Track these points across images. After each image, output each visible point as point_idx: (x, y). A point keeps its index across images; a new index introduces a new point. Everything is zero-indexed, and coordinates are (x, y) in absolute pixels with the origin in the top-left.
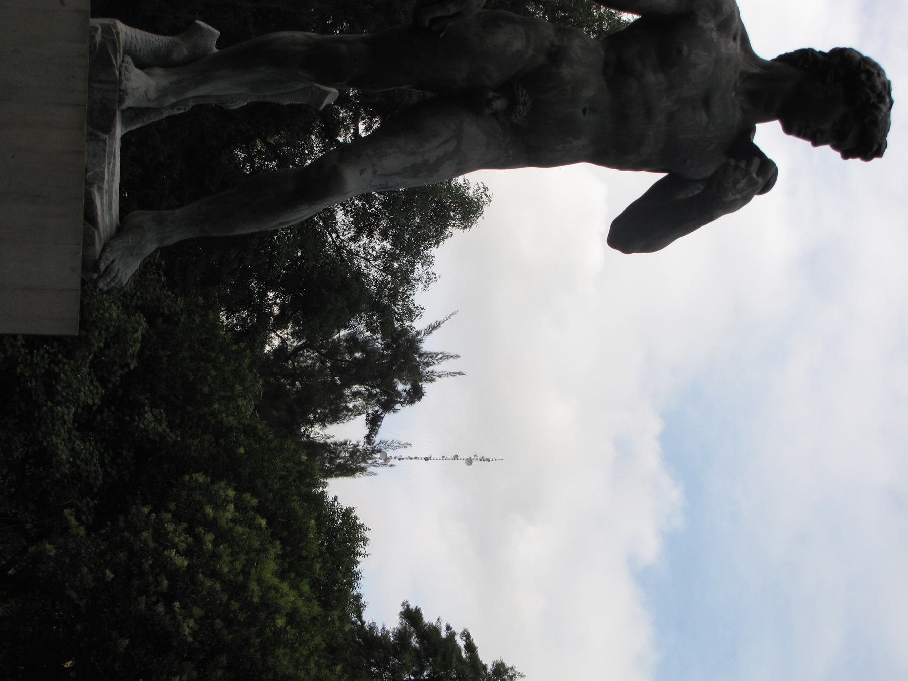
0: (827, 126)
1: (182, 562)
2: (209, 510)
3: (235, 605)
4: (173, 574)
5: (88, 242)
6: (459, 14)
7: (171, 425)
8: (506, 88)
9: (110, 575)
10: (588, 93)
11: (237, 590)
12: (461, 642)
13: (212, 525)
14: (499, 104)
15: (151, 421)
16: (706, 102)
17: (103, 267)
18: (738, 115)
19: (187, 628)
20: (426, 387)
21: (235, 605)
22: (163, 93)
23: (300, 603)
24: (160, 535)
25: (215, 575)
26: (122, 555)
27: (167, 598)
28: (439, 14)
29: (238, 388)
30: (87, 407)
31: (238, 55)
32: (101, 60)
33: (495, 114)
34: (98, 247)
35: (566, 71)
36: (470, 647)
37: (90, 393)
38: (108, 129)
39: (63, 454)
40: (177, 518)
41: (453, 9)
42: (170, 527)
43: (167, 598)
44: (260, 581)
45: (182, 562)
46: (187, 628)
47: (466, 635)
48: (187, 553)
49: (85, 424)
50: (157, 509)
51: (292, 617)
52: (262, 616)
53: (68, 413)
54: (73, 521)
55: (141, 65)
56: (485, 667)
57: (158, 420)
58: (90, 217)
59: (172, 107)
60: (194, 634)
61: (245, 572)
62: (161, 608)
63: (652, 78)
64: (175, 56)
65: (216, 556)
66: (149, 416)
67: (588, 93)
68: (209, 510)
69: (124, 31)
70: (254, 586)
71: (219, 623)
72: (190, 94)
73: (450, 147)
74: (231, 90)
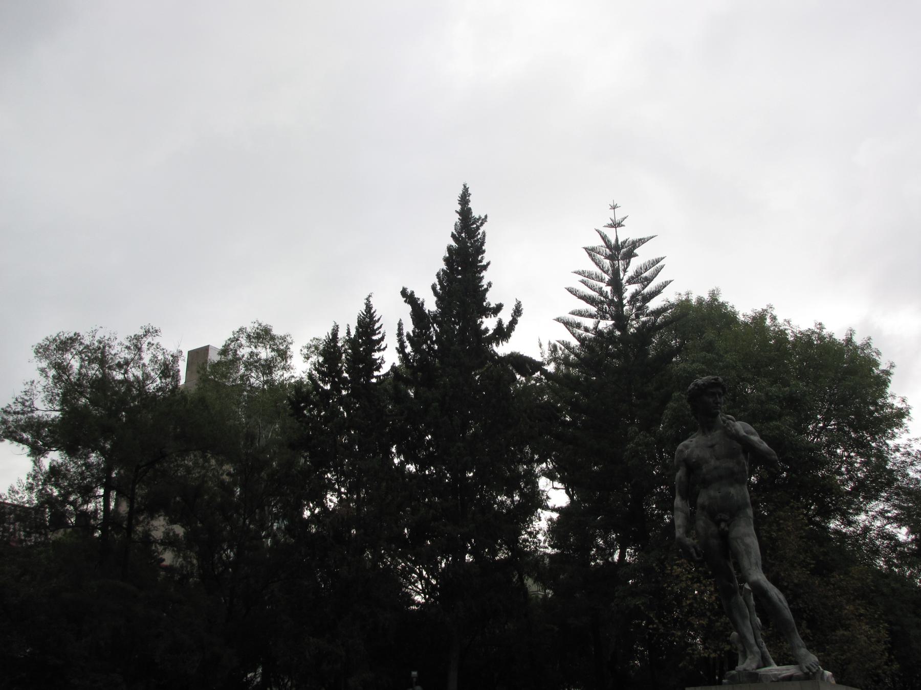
0: (711, 400)
6: (694, 547)
8: (718, 523)
10: (712, 493)
14: (723, 525)
16: (712, 446)
17: (806, 670)
22: (752, 652)
28: (695, 555)
33: (728, 525)
34: (800, 673)
35: (706, 503)
38: (757, 674)
41: (693, 550)
58: (790, 678)
59: (760, 647)
63: (704, 470)
64: (742, 649)
72: (752, 641)
73: (739, 541)
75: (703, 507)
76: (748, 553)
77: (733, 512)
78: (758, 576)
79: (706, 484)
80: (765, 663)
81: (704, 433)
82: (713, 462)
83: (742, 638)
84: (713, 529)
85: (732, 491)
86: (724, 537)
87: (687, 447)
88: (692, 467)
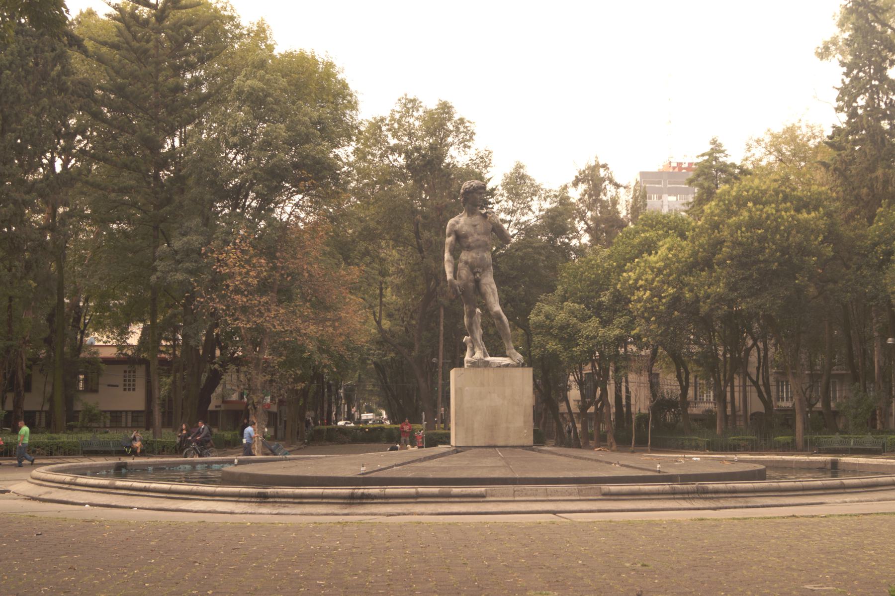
1: (648, 293)
2: (631, 282)
3: (665, 272)
4: (653, 296)
5: (513, 366)
7: (607, 289)
8: (475, 274)
9: (653, 319)
10: (474, 255)
11: (660, 271)
12: (700, 160)
13: (636, 281)
15: (605, 297)
16: (475, 226)
18: (478, 217)
19: (671, 291)
20: (601, 164)
21: (665, 272)
22: (480, 349)
23: (666, 246)
24: (640, 300)
25: (653, 280)
26: (646, 315)
27: (661, 298)
29: (593, 262)
30: (601, 323)
31: (471, 332)
32: (474, 364)
35: (470, 260)
36: (703, 155)
37: (595, 322)
38: (488, 362)
39: (617, 332)
40: (633, 294)
42: (636, 297)
43: (661, 298)
44: (656, 263)
45: (648, 293)
46: (671, 291)
47: (698, 157)
48: (645, 290)
49: (605, 323)
50: (630, 302)
51: (670, 249)
52: (668, 262)
53: (601, 331)
54: (635, 332)
55: (474, 354)
56: (712, 149)
57: (605, 295)
58: (507, 366)
60: (674, 287)
61: (652, 269)
62: (664, 301)
63: (470, 240)
65: (646, 280)
66: (603, 299)
67: (474, 255)
68: (631, 282)
69: (467, 357)
70: (657, 265)
71: (671, 278)
74: (479, 333)
75: (466, 263)
76: (494, 294)
77: (484, 268)
78: (497, 308)
79: (469, 248)
80: (485, 356)
81: (468, 216)
82: (476, 236)
83: (473, 341)
84: (472, 277)
85: (485, 255)
86: (477, 282)
87: (457, 223)
88: (459, 237)
